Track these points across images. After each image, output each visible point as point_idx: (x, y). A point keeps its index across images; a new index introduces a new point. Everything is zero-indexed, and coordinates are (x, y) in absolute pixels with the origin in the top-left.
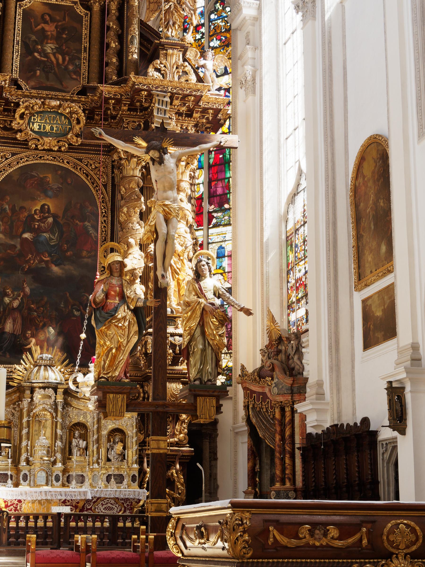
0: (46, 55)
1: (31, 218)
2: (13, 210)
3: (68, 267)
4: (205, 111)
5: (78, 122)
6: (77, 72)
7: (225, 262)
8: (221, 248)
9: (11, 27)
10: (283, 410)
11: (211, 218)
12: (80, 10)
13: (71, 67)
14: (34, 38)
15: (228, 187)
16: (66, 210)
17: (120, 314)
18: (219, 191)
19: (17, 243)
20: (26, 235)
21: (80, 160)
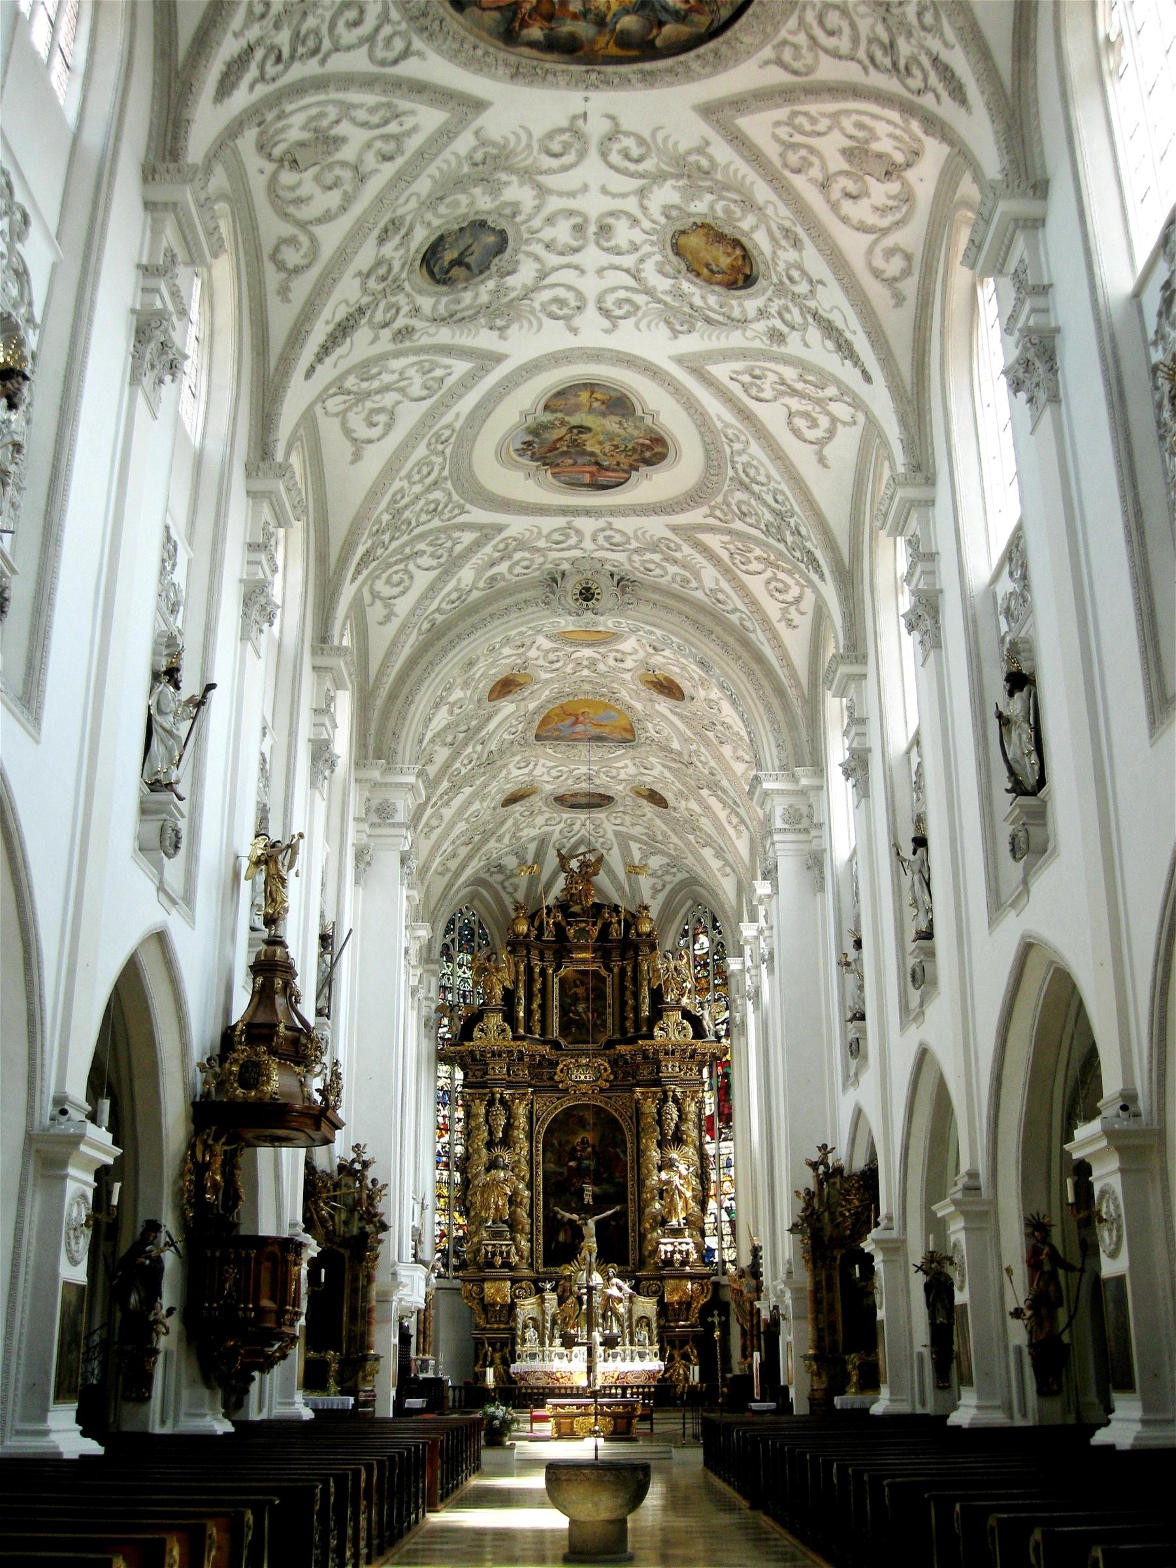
0: (579, 1015)
1: (574, 1149)
2: (560, 1144)
3: (605, 1186)
4: (704, 1054)
5: (605, 1070)
6: (604, 1025)
7: (732, 1172)
8: (729, 1159)
9: (550, 996)
10: (752, 1303)
11: (721, 1133)
12: (604, 972)
13: (599, 1022)
14: (569, 1001)
15: (730, 1108)
16: (600, 1141)
17: (570, 1301)
18: (726, 1111)
19: (565, 1170)
20: (572, 1164)
21: (610, 1098)
